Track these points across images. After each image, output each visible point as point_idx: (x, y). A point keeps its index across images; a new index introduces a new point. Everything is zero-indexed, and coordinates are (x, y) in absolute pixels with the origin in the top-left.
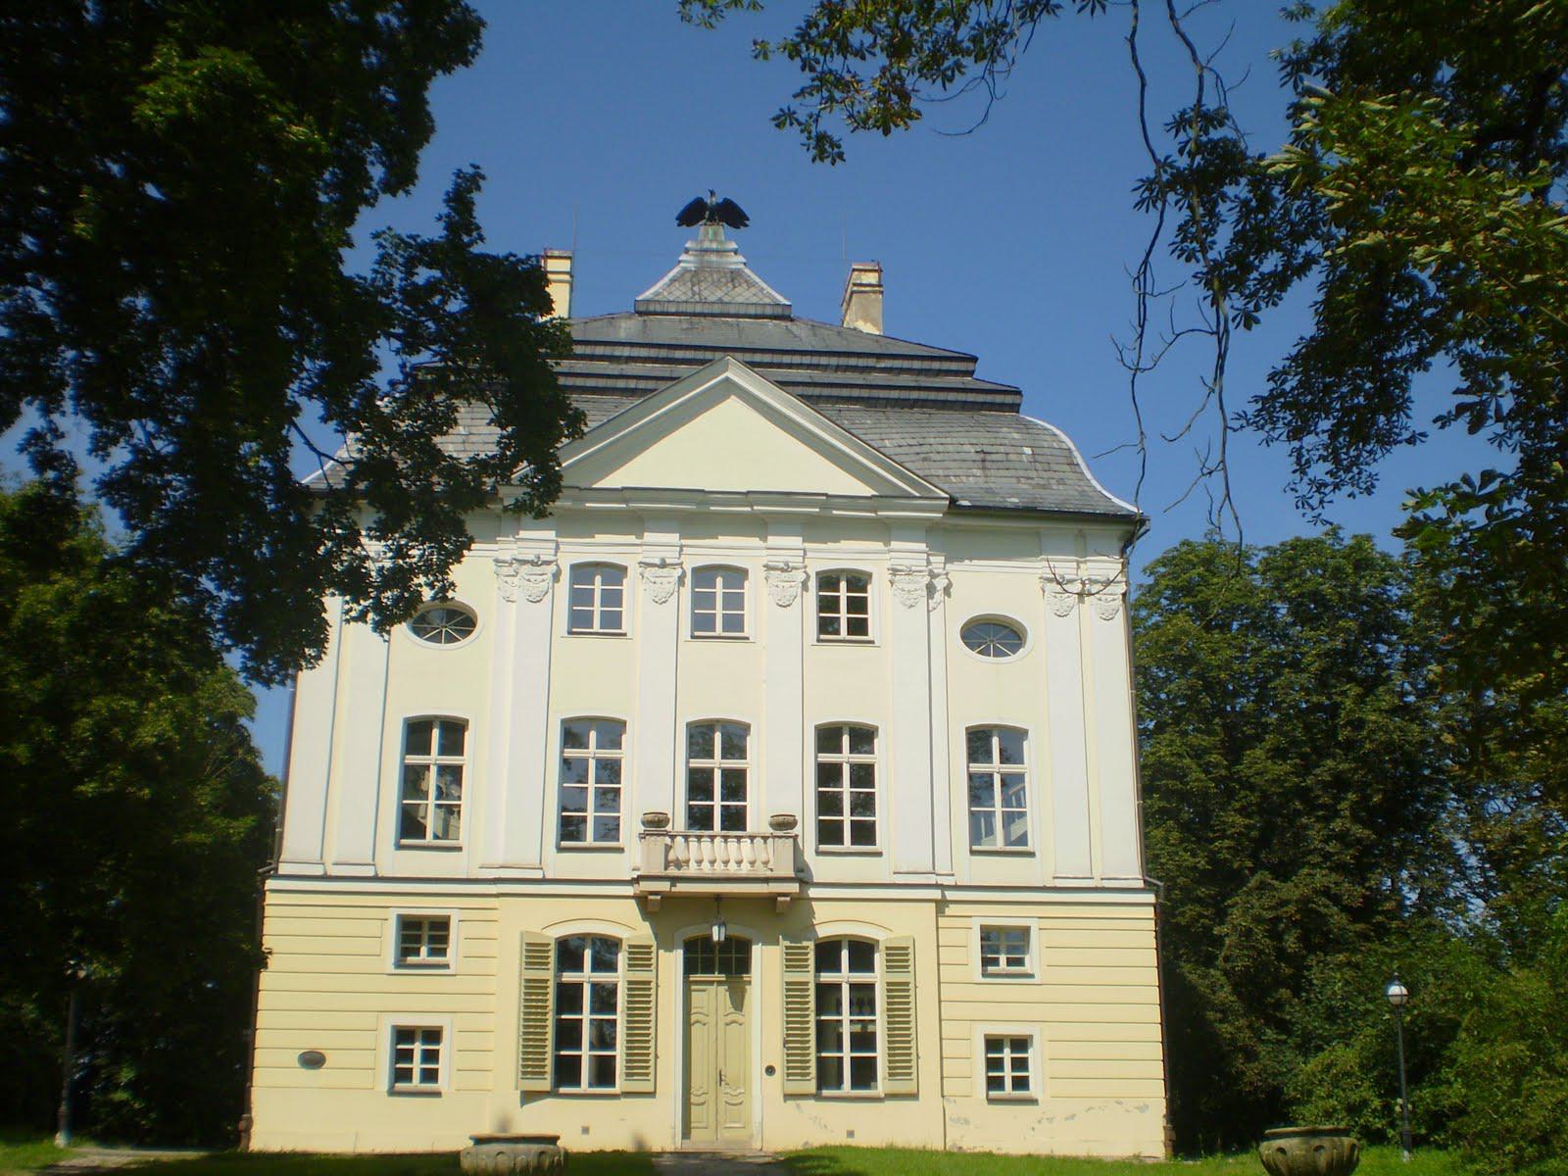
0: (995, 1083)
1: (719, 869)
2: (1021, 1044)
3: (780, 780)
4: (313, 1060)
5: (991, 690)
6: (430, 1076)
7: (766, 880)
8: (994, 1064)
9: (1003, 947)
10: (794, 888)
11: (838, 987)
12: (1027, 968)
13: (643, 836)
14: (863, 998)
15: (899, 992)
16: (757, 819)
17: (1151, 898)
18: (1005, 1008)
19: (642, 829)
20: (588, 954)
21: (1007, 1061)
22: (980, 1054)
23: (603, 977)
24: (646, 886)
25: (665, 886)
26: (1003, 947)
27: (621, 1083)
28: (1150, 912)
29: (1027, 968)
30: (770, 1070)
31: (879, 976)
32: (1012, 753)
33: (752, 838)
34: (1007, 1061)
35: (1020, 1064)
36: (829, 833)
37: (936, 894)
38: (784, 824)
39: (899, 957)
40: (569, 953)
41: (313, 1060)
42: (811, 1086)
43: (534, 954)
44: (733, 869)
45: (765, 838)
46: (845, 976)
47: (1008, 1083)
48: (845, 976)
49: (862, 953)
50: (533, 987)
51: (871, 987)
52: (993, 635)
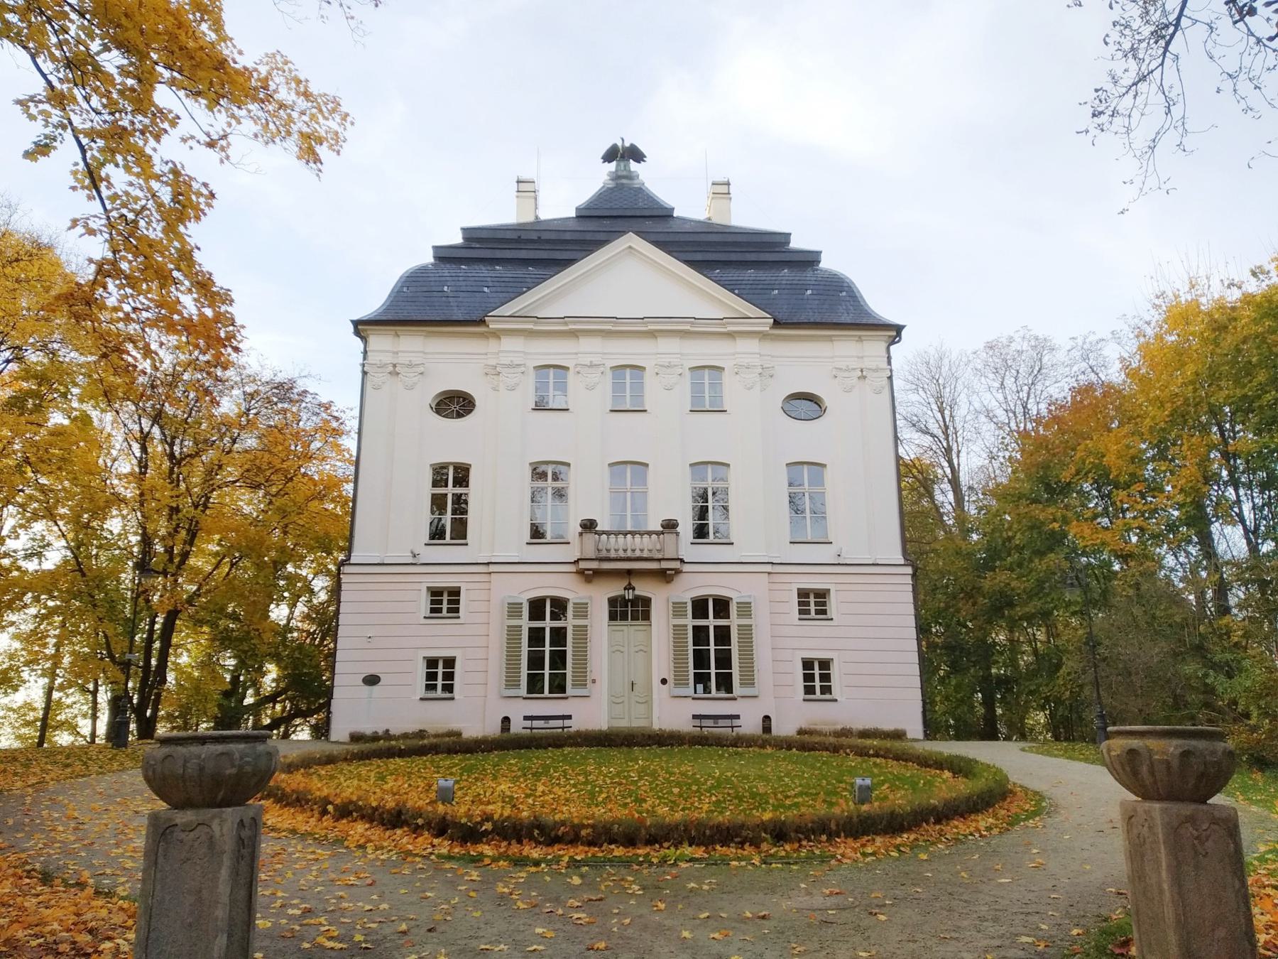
0: (809, 690)
2: (825, 664)
3: (670, 499)
4: (372, 680)
5: (804, 440)
6: (449, 688)
7: (659, 560)
8: (808, 678)
9: (814, 603)
10: (676, 565)
12: (829, 616)
13: (581, 534)
14: (723, 635)
15: (746, 631)
18: (815, 640)
19: (580, 529)
21: (817, 676)
22: (799, 672)
24: (583, 565)
25: (594, 565)
26: (814, 603)
28: (909, 580)
29: (829, 616)
30: (664, 681)
31: (734, 622)
32: (818, 480)
33: (650, 533)
34: (817, 676)
35: (825, 678)
36: (701, 532)
38: (670, 526)
39: (745, 609)
40: (537, 607)
41: (372, 680)
43: (514, 610)
46: (711, 622)
47: (818, 690)
48: (711, 622)
49: (722, 606)
50: (514, 632)
52: (805, 404)
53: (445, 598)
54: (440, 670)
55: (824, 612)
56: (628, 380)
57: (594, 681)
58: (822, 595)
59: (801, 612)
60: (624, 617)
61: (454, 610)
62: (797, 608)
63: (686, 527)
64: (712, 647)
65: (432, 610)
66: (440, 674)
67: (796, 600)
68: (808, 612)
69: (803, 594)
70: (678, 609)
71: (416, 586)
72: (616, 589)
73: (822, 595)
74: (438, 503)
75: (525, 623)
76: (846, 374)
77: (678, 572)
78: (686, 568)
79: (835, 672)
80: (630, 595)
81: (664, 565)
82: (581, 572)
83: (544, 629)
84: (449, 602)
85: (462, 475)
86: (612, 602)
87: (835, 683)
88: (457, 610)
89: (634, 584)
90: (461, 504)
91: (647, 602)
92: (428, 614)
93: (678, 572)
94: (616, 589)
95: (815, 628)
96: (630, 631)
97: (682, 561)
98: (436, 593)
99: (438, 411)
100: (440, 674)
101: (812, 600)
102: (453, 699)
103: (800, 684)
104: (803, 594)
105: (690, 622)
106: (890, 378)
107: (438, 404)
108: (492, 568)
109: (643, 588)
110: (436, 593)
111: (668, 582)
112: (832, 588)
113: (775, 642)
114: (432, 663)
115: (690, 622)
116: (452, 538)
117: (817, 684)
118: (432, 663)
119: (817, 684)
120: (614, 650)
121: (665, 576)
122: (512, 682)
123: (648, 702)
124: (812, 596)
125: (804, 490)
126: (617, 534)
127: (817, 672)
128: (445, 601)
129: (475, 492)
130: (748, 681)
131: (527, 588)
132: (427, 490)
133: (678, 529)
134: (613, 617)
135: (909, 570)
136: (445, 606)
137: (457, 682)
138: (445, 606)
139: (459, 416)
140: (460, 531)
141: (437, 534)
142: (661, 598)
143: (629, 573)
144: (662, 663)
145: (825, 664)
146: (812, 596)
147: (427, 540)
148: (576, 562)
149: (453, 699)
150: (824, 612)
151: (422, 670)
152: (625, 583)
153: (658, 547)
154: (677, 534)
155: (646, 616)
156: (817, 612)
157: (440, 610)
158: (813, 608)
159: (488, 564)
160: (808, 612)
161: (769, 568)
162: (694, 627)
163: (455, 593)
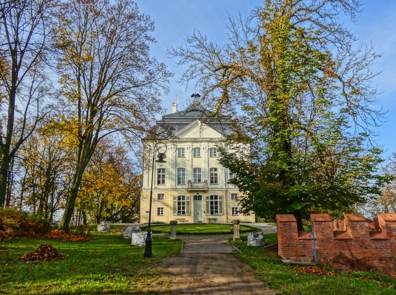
0: (233, 213)
6: (162, 214)
8: (233, 211)
10: (207, 189)
14: (216, 203)
15: (221, 202)
16: (202, 181)
20: (181, 197)
24: (188, 189)
25: (191, 189)
27: (186, 214)
36: (212, 182)
37: (225, 189)
38: (206, 181)
40: (179, 198)
42: (210, 214)
46: (214, 200)
51: (217, 202)
63: (209, 182)
64: (214, 205)
65: (159, 198)
72: (195, 194)
75: (177, 200)
77: (207, 190)
78: (209, 190)
80: (198, 195)
81: (205, 189)
82: (188, 191)
86: (194, 196)
91: (201, 196)
94: (195, 194)
105: (210, 200)
109: (200, 194)
115: (210, 200)
118: (159, 209)
121: (204, 192)
130: (221, 212)
131: (176, 194)
134: (194, 199)
138: (161, 197)
144: (204, 209)
148: (187, 189)
155: (201, 199)
158: (234, 197)
163: (163, 195)
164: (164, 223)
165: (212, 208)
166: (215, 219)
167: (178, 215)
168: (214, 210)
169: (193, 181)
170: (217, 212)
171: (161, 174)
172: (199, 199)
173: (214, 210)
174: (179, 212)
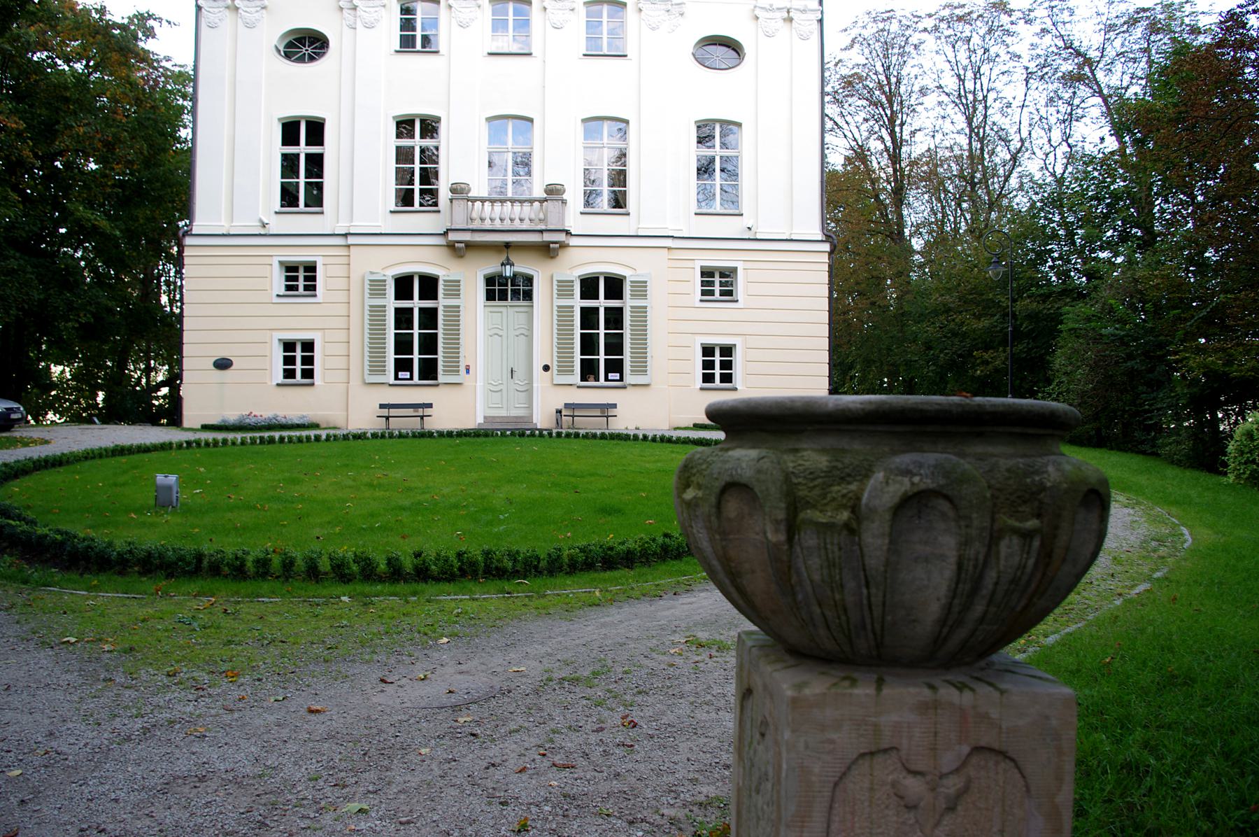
1: (507, 225)
2: (727, 351)
4: (223, 364)
6: (308, 374)
7: (541, 231)
8: (708, 365)
9: (719, 283)
10: (561, 237)
11: (597, 309)
13: (451, 200)
14: (615, 318)
15: (641, 312)
17: (827, 247)
18: (718, 323)
22: (699, 358)
23: (428, 304)
25: (467, 237)
26: (719, 283)
27: (441, 378)
30: (546, 368)
31: (628, 303)
33: (531, 201)
35: (727, 365)
38: (554, 192)
39: (641, 288)
40: (403, 286)
41: (223, 364)
43: (377, 287)
44: (517, 225)
45: (542, 201)
48: (602, 303)
49: (615, 286)
50: (378, 311)
53: (301, 274)
54: (299, 354)
55: (730, 293)
56: (511, 17)
57: (468, 372)
58: (728, 275)
59: (704, 293)
60: (503, 297)
61: (311, 289)
62: (699, 288)
64: (602, 331)
65: (289, 288)
66: (299, 359)
67: (698, 279)
68: (712, 293)
69: (707, 273)
70: (564, 288)
71: (267, 260)
72: (491, 265)
73: (728, 275)
74: (289, 165)
75: (391, 303)
76: (770, 15)
77: (563, 246)
78: (573, 241)
79: (738, 359)
80: (508, 272)
82: (451, 246)
83: (411, 310)
84: (306, 279)
85: (316, 130)
86: (490, 281)
87: (738, 371)
88: (314, 288)
89: (512, 259)
90: (316, 164)
91: (529, 280)
92: (282, 291)
93: (563, 246)
94: (491, 265)
95: (719, 310)
96: (510, 311)
97: (568, 233)
98: (290, 269)
99: (288, 56)
100: (299, 359)
101: (717, 280)
102: (313, 384)
103: (699, 371)
104: (707, 273)
105: (578, 303)
106: (821, 21)
107: (287, 46)
108: (351, 240)
109: (522, 265)
110: (290, 269)
111: (552, 257)
112: (740, 267)
113: (671, 328)
114: (289, 346)
115: (578, 303)
116: (306, 205)
117: (717, 371)
118: (289, 346)
119: (717, 371)
120: (494, 333)
121: (547, 251)
122: (377, 368)
123: (529, 391)
124: (717, 275)
125: (716, 153)
126: (493, 201)
127: (717, 359)
128: (300, 277)
129: (330, 149)
130: (641, 368)
132: (277, 149)
133: (565, 197)
134: (490, 296)
135: (827, 247)
136: (301, 283)
137: (317, 367)
138: (301, 283)
139: (312, 59)
140: (316, 198)
141: (289, 197)
142: (543, 276)
143: (508, 245)
144: (543, 348)
145: (727, 351)
146: (717, 275)
147: (278, 207)
148: (445, 234)
149: (313, 384)
150: (730, 293)
151: (279, 354)
152: (503, 258)
153: (542, 216)
154: (564, 202)
155: (528, 296)
156: (723, 293)
157: (295, 288)
158: (717, 289)
159: (346, 235)
160: (712, 293)
161: (669, 243)
162: (582, 309)
163: (311, 268)
164: (316, 426)
165: (588, 344)
166: (606, 409)
167: (398, 382)
168: (602, 357)
169: (480, 188)
170: (615, 366)
171: (303, 149)
172: (516, 294)
173: (602, 357)
174: (403, 366)
